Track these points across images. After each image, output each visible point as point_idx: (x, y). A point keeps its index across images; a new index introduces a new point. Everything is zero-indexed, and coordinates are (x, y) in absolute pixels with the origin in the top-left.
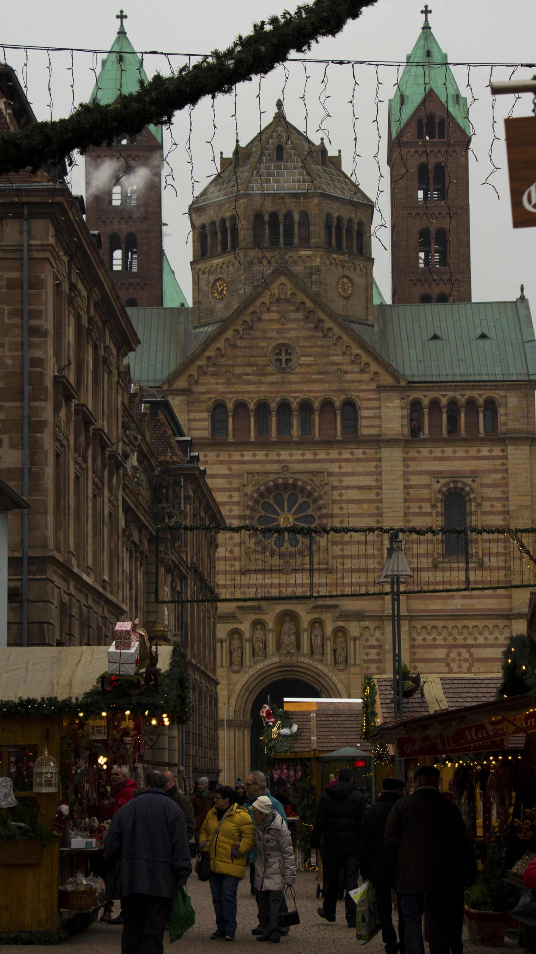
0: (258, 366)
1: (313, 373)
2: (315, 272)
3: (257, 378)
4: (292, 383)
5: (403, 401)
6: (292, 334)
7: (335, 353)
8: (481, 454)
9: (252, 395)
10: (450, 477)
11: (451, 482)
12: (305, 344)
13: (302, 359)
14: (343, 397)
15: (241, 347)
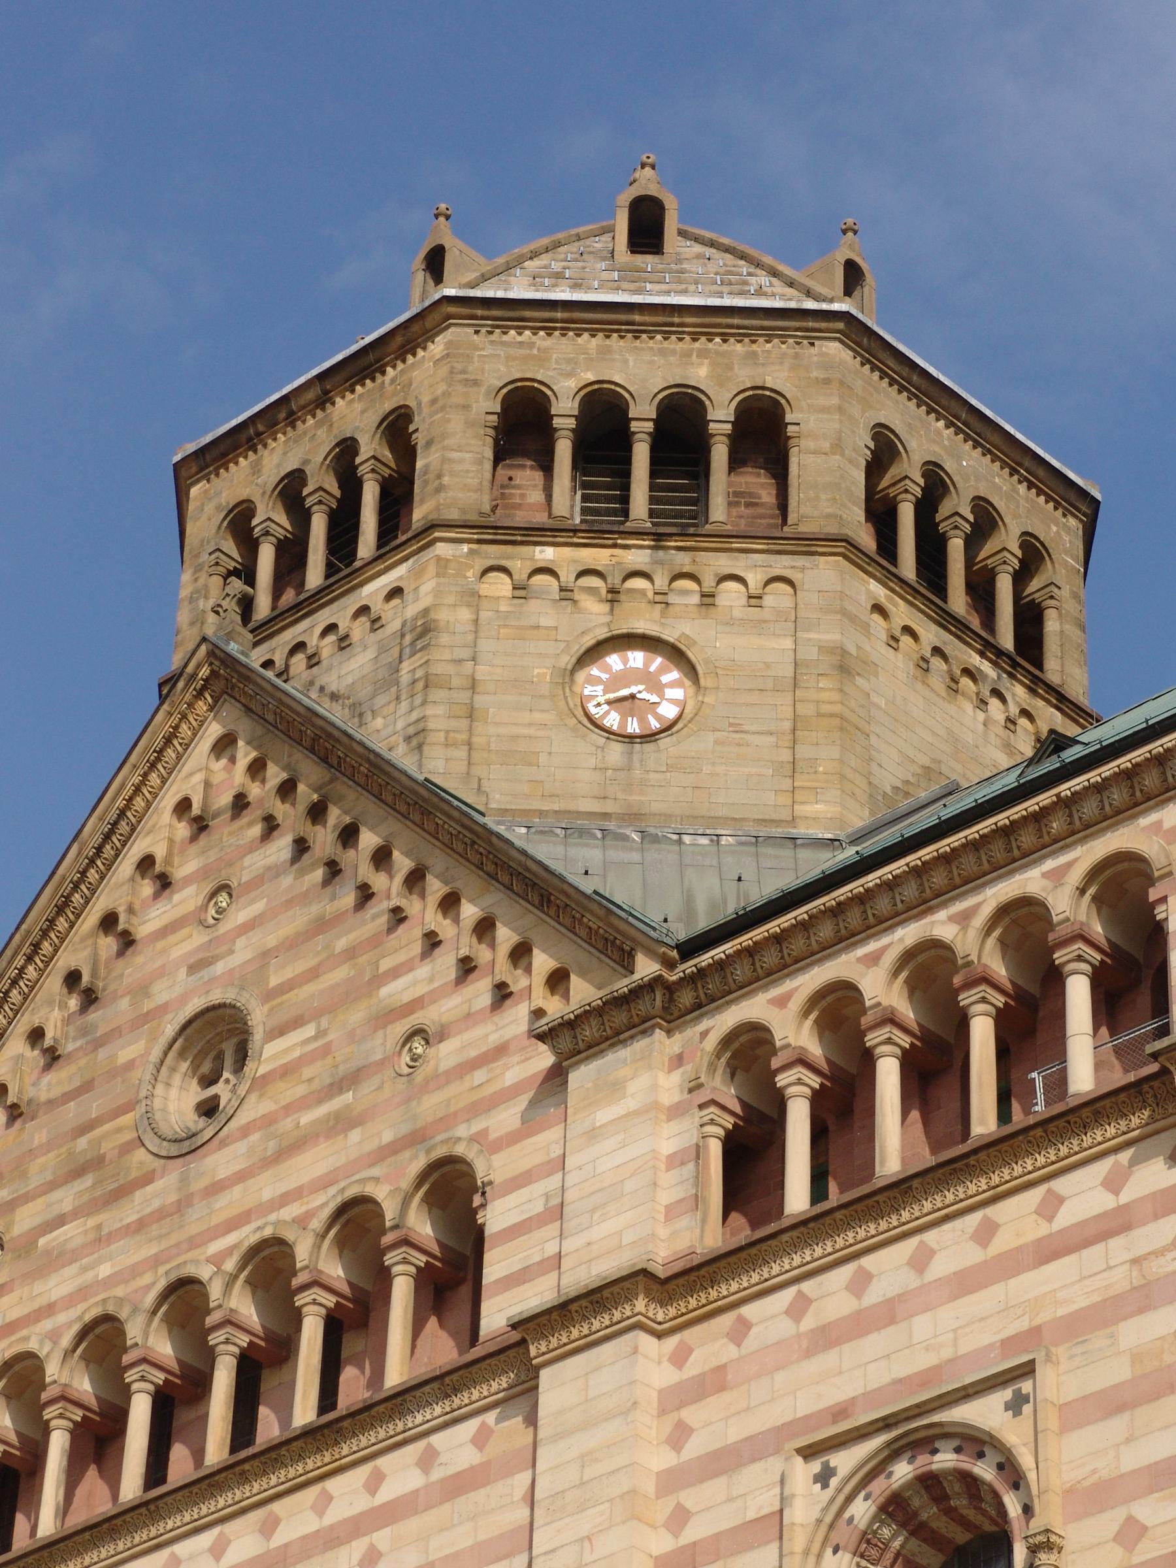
0: (96, 1163)
1: (303, 1104)
2: (413, 643)
3: (91, 1222)
4: (216, 1188)
5: (676, 1077)
6: (243, 952)
7: (401, 957)
8: (1066, 1217)
9: (62, 1318)
10: (885, 1423)
11: (893, 1453)
12: (288, 973)
13: (271, 1049)
14: (418, 1164)
15: (50, 1102)
